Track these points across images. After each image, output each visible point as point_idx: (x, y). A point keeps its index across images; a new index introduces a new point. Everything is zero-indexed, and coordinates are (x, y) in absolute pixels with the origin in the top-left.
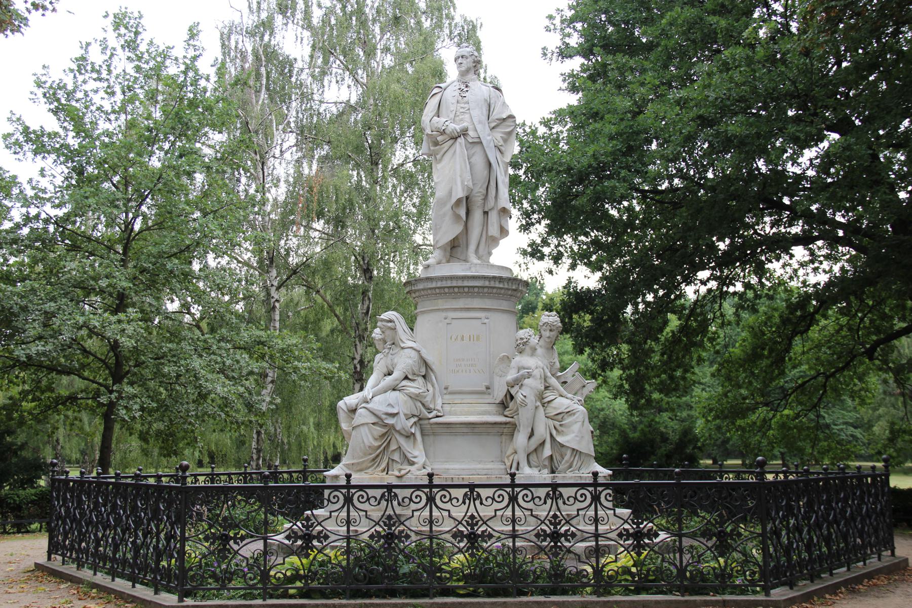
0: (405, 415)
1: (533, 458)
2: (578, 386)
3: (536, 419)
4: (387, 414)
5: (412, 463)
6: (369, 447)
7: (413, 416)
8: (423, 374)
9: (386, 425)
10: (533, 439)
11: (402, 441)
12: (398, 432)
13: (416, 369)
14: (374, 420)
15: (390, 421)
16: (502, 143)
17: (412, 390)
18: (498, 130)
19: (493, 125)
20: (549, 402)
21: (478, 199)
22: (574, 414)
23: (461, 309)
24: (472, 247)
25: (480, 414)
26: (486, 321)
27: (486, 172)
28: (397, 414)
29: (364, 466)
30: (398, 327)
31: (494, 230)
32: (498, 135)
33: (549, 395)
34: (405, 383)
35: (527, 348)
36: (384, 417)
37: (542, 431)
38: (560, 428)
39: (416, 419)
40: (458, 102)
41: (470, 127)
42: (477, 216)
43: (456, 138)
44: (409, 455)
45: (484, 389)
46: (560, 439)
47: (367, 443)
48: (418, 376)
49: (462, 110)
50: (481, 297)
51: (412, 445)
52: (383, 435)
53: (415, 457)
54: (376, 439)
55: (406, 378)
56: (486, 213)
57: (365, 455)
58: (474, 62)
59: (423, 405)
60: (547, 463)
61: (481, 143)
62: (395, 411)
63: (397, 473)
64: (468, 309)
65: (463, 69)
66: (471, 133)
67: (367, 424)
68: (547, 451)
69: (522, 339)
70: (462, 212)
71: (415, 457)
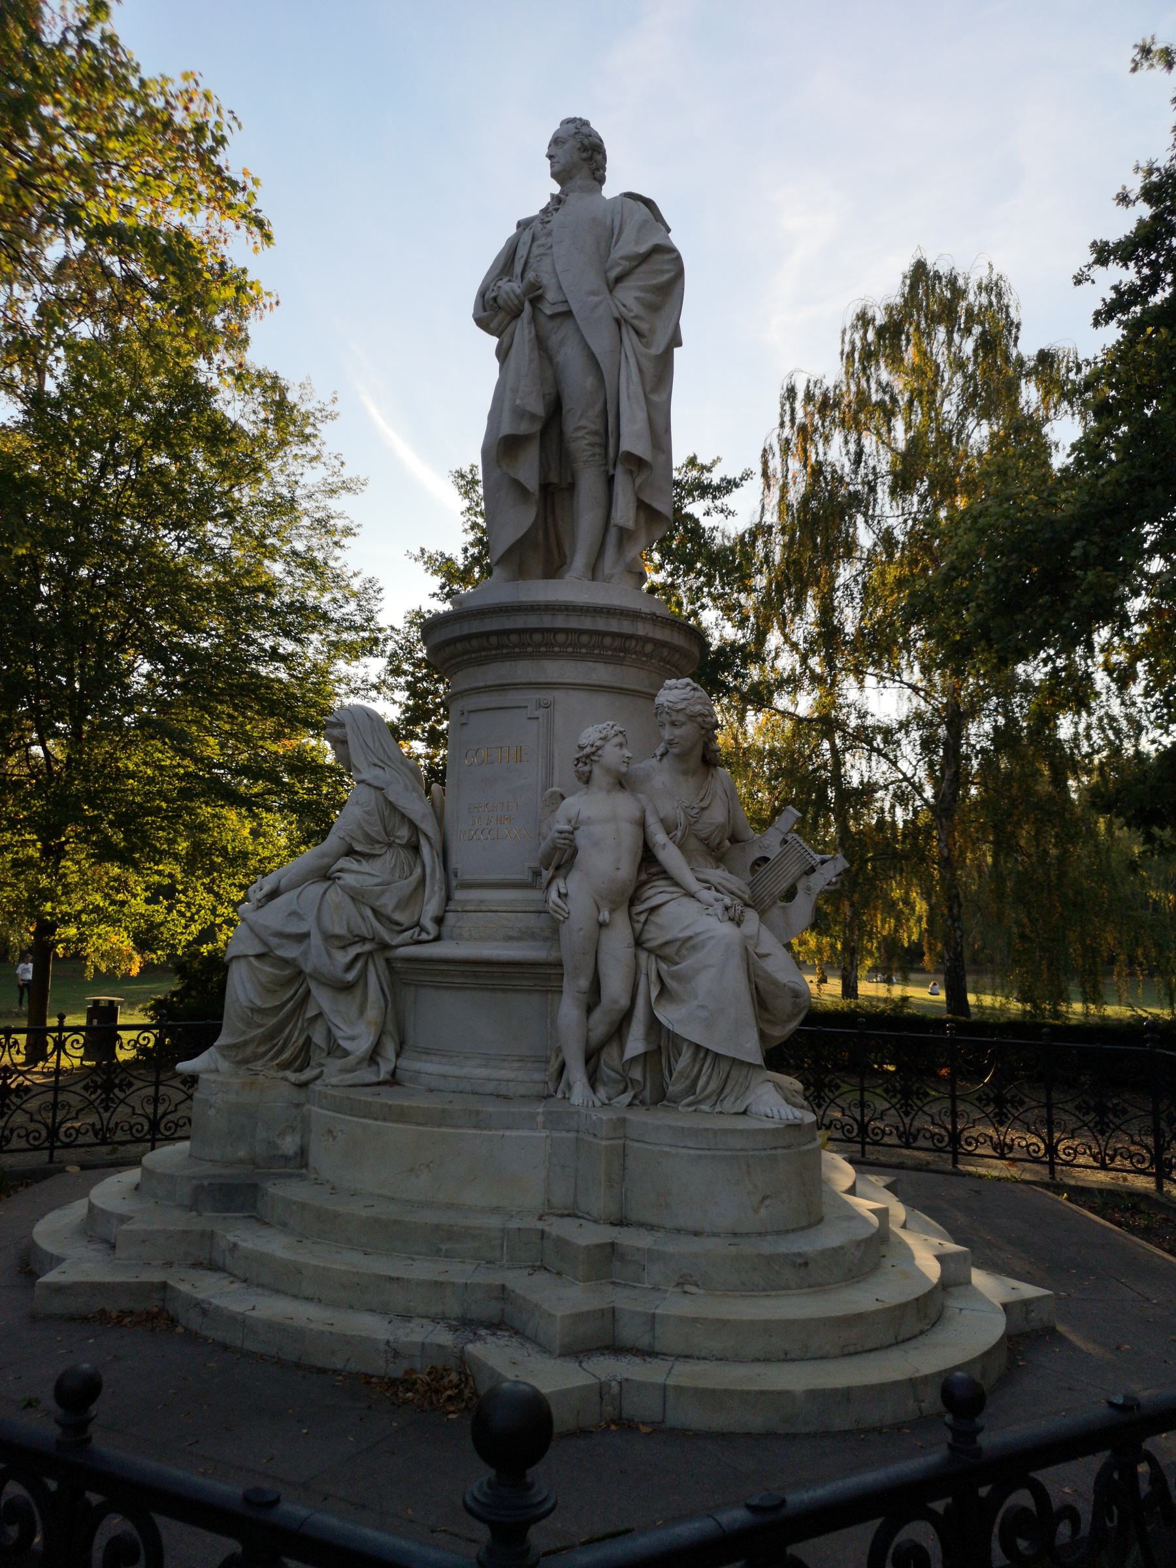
0: (328, 937)
1: (610, 1057)
2: (795, 869)
3: (602, 956)
4: (280, 935)
5: (346, 1053)
6: (252, 1010)
7: (363, 940)
8: (404, 841)
9: (285, 962)
10: (597, 1014)
11: (322, 999)
12: (311, 976)
13: (375, 830)
14: (259, 949)
15: (290, 952)
16: (637, 309)
17: (348, 879)
18: (630, 282)
19: (613, 274)
20: (653, 910)
21: (581, 443)
22: (703, 944)
23: (478, 690)
24: (580, 561)
25: (511, 938)
26: (539, 713)
27: (590, 382)
28: (305, 936)
29: (249, 1050)
30: (351, 739)
31: (624, 513)
32: (629, 296)
33: (658, 893)
34: (343, 863)
35: (597, 771)
36: (274, 941)
37: (615, 987)
38: (671, 984)
39: (368, 947)
40: (534, 239)
41: (547, 280)
42: (589, 483)
43: (516, 314)
44: (337, 1033)
45: (527, 876)
46: (667, 1015)
47: (245, 1003)
48: (390, 845)
49: (541, 250)
50: (531, 656)
51: (354, 1010)
52: (289, 982)
53: (352, 1038)
54: (269, 991)
55: (350, 852)
56: (610, 481)
57: (249, 1024)
58: (584, 148)
59: (374, 911)
60: (637, 1074)
61: (568, 314)
62: (302, 928)
63: (308, 1074)
64: (502, 688)
65: (558, 167)
66: (551, 296)
67: (246, 956)
68: (635, 1044)
69: (581, 748)
70: (528, 471)
71: (352, 1038)
